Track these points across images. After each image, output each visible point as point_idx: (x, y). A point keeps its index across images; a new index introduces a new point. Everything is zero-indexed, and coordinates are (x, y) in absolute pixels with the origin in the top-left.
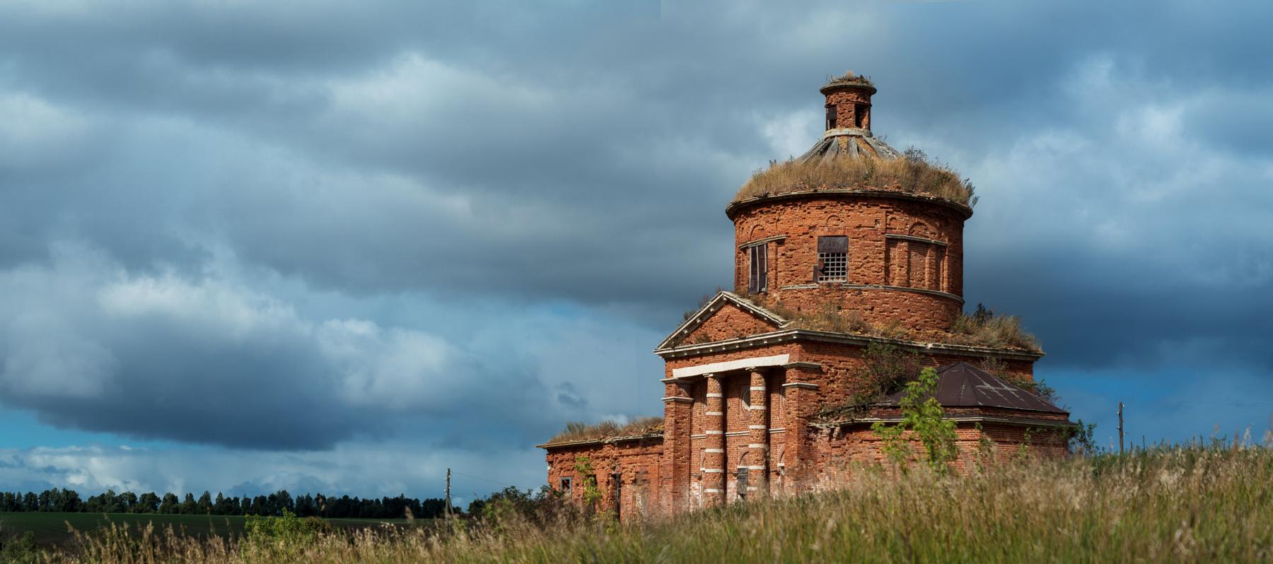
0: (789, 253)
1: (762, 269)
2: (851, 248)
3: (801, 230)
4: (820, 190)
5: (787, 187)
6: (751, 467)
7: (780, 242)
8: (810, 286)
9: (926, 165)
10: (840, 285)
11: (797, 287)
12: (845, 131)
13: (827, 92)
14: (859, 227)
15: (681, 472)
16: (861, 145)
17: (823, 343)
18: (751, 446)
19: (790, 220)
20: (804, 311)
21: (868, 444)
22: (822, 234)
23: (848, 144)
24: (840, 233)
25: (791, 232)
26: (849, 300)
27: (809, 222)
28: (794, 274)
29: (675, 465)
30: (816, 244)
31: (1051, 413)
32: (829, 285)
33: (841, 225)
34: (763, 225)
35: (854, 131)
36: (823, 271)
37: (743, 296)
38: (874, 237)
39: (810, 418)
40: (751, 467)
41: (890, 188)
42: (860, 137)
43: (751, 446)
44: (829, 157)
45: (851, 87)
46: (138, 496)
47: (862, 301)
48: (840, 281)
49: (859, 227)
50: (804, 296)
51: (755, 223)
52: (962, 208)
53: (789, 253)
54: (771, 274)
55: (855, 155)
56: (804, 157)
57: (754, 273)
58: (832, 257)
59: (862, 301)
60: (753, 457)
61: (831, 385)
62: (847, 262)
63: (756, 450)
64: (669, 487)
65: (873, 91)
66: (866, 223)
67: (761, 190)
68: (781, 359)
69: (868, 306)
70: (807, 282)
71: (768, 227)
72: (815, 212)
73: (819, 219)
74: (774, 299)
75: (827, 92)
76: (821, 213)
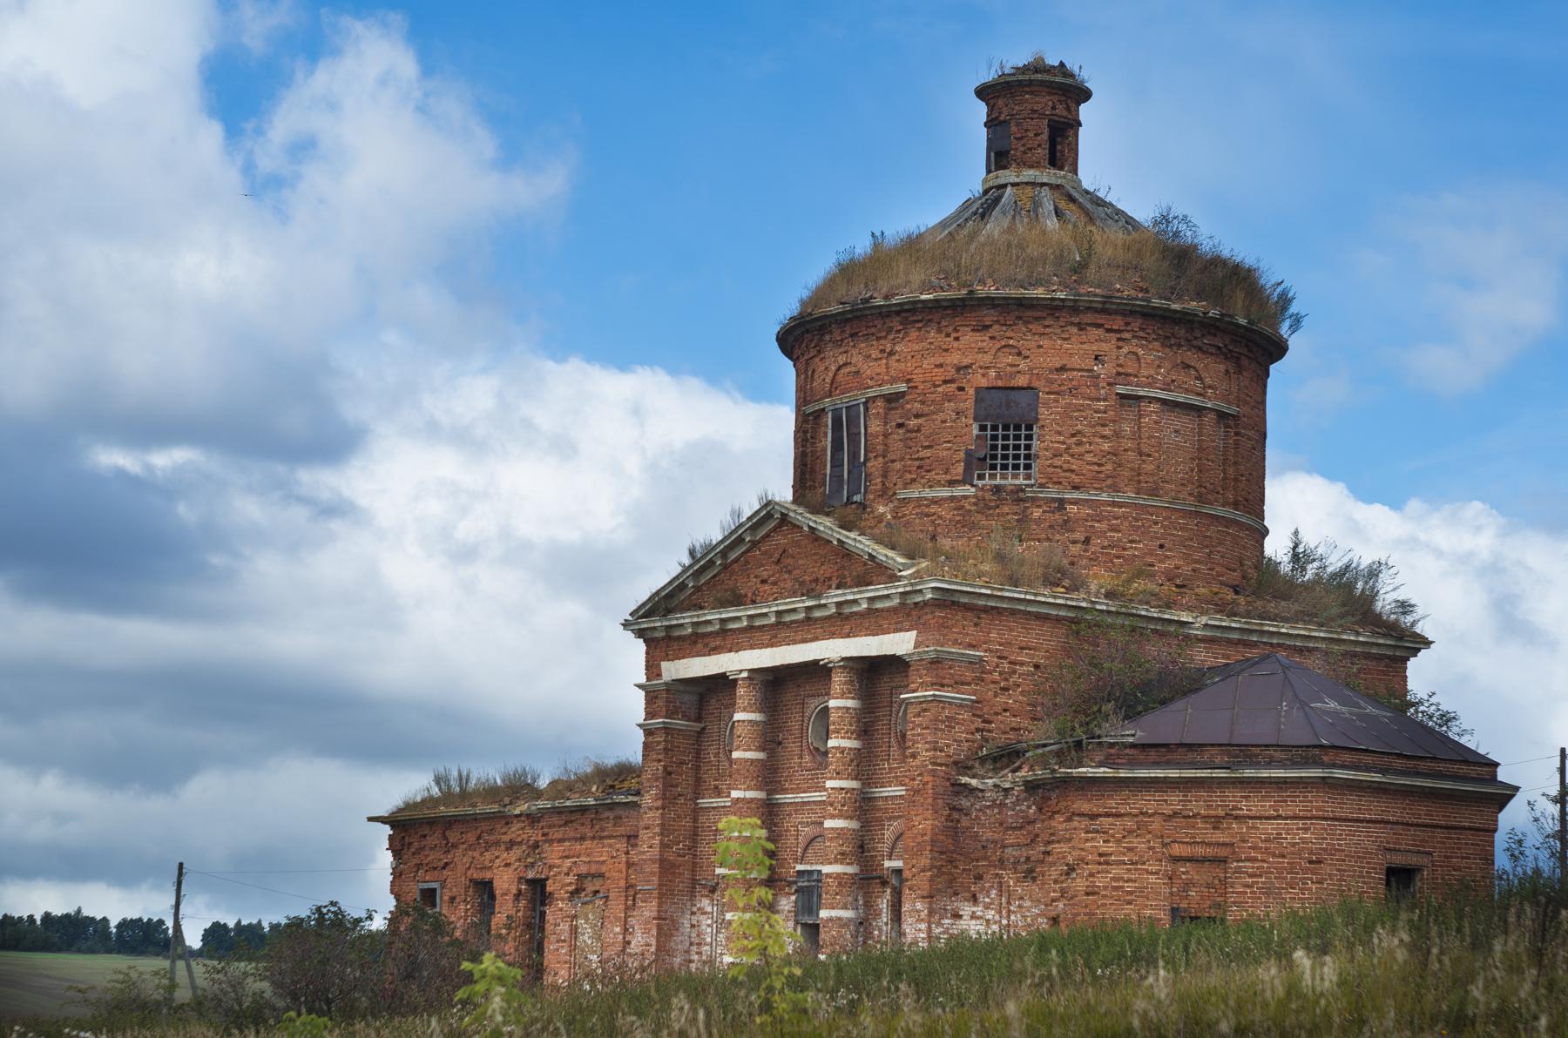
0: (913, 423)
1: (854, 455)
2: (1043, 412)
3: (939, 375)
4: (981, 291)
5: (914, 286)
6: (826, 869)
7: (892, 399)
8: (959, 491)
9: (1195, 247)
10: (1020, 489)
11: (929, 493)
12: (1029, 174)
13: (983, 92)
14: (1063, 369)
15: (684, 876)
16: (1062, 204)
17: (987, 610)
18: (828, 824)
19: (916, 358)
20: (946, 543)
21: (1085, 822)
22: (984, 383)
23: (1037, 204)
24: (1021, 381)
25: (918, 378)
26: (1038, 521)
27: (955, 358)
28: (923, 467)
29: (662, 861)
30: (969, 405)
31: (1466, 762)
32: (997, 489)
33: (1023, 365)
34: (871, 367)
35: (1047, 175)
36: (977, 463)
37: (815, 510)
38: (1092, 392)
39: (963, 767)
40: (826, 869)
41: (1125, 291)
42: (1058, 187)
43: (828, 824)
44: (994, 227)
45: (1042, 83)
46: (113, 923)
47: (1067, 525)
48: (1021, 481)
49: (1063, 369)
50: (944, 512)
51: (842, 360)
52: (1268, 339)
53: (913, 423)
54: (875, 465)
55: (1052, 223)
56: (943, 224)
57: (837, 464)
58: (1006, 428)
59: (1067, 525)
60: (833, 847)
61: (1001, 699)
62: (1035, 443)
63: (840, 833)
64: (648, 910)
65: (1085, 95)
66: (1075, 362)
67: (858, 291)
68: (900, 643)
69: (1079, 535)
70: (951, 483)
71: (868, 369)
72: (969, 338)
73: (978, 356)
74: (880, 518)
75: (983, 92)
76: (982, 339)
